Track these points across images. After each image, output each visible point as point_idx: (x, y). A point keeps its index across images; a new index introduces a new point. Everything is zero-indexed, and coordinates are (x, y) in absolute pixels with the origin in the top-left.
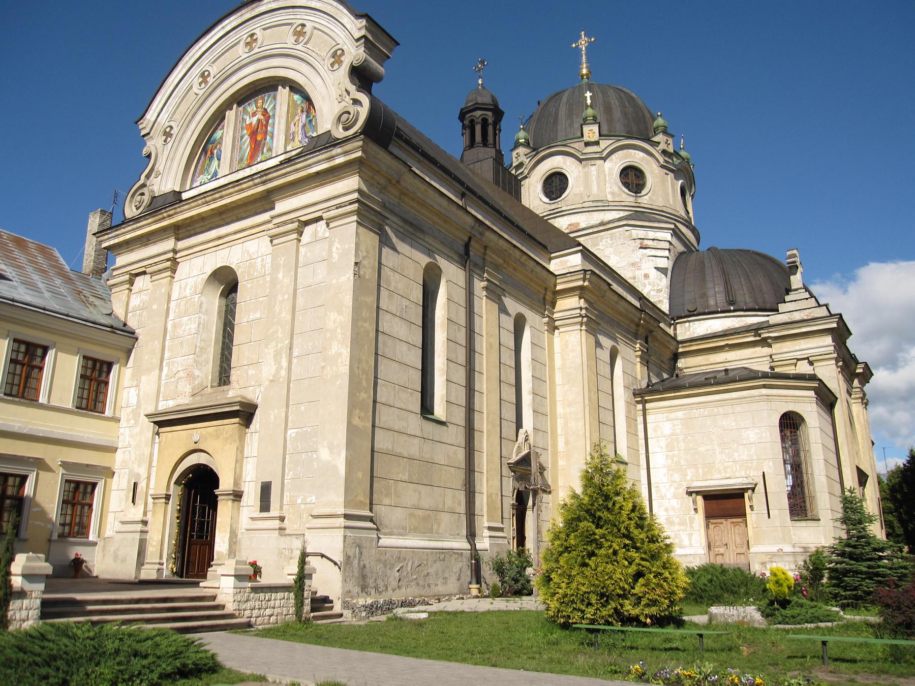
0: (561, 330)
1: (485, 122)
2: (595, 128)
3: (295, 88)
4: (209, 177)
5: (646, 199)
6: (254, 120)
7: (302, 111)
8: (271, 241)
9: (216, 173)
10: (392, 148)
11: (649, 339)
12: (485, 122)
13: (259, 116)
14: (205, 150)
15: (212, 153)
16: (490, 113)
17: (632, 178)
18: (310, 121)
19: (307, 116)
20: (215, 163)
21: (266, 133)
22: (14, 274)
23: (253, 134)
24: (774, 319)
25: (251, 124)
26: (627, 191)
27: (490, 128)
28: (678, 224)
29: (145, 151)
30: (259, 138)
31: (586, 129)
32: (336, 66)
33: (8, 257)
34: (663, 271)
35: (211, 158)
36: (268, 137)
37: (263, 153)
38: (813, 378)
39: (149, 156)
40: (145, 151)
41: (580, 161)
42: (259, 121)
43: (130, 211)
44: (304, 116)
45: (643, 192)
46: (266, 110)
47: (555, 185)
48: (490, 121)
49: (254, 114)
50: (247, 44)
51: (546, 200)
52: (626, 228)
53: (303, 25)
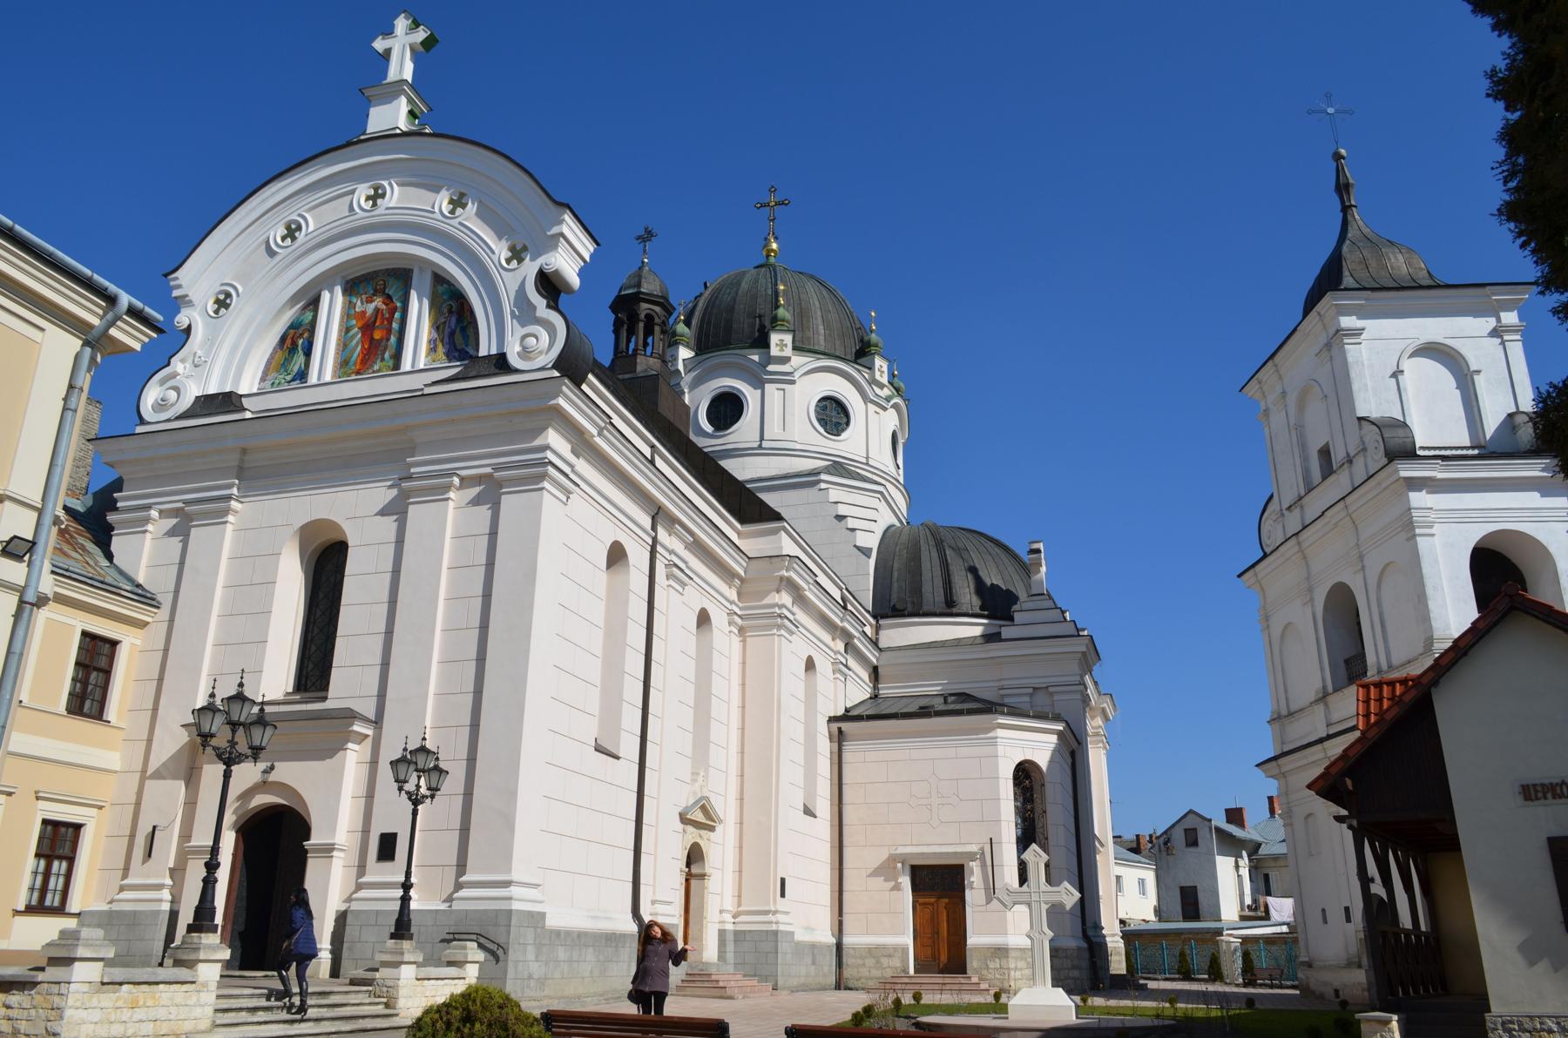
2: (788, 338)
3: (440, 280)
4: (289, 378)
5: (849, 445)
6: (370, 308)
7: (450, 312)
9: (302, 376)
10: (584, 387)
12: (649, 318)
14: (283, 339)
15: (294, 344)
16: (657, 309)
17: (833, 415)
18: (463, 330)
19: (459, 320)
21: (389, 331)
23: (368, 328)
25: (364, 313)
28: (889, 486)
30: (377, 335)
31: (775, 338)
32: (514, 263)
34: (866, 552)
35: (293, 349)
36: (393, 339)
37: (383, 359)
39: (188, 330)
42: (377, 310)
44: (454, 319)
45: (844, 435)
50: (368, 198)
52: (823, 486)
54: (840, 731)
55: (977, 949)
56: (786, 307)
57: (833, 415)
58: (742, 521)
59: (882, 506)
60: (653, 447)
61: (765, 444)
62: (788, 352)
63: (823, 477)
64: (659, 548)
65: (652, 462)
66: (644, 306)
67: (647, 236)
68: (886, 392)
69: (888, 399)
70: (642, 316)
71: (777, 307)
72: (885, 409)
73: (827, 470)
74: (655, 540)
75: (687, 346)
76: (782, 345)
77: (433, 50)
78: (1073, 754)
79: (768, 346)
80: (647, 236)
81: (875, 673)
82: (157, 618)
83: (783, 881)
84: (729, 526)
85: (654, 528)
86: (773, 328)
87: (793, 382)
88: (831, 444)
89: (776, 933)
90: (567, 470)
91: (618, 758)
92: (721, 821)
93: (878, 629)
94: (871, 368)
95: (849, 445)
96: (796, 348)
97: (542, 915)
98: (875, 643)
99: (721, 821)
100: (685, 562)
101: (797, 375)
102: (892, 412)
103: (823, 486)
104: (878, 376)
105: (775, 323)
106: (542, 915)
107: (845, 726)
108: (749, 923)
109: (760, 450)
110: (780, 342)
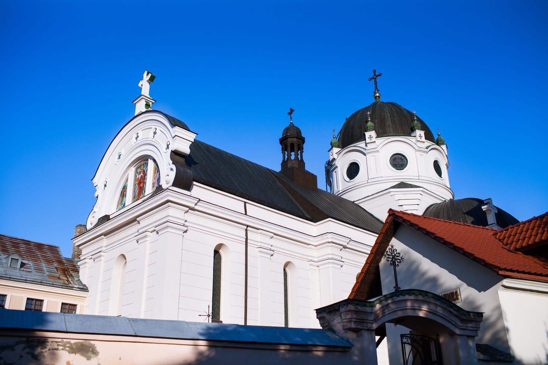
0: (321, 267)
1: (292, 145)
3: (155, 161)
6: (140, 175)
8: (138, 242)
12: (292, 145)
13: (142, 174)
16: (295, 140)
17: (399, 162)
20: (124, 199)
22: (32, 265)
26: (394, 169)
29: (96, 195)
31: (367, 134)
33: (31, 256)
35: (123, 196)
40: (96, 195)
41: (365, 154)
42: (141, 176)
43: (89, 227)
47: (353, 170)
48: (295, 145)
49: (140, 173)
51: (348, 179)
52: (392, 194)
60: (245, 203)
62: (374, 139)
64: (248, 241)
66: (289, 140)
67: (292, 111)
70: (289, 144)
74: (247, 239)
75: (338, 147)
76: (370, 137)
77: (154, 81)
80: (292, 111)
82: (89, 295)
86: (366, 131)
96: (379, 136)
101: (378, 149)
103: (392, 194)
109: (368, 183)
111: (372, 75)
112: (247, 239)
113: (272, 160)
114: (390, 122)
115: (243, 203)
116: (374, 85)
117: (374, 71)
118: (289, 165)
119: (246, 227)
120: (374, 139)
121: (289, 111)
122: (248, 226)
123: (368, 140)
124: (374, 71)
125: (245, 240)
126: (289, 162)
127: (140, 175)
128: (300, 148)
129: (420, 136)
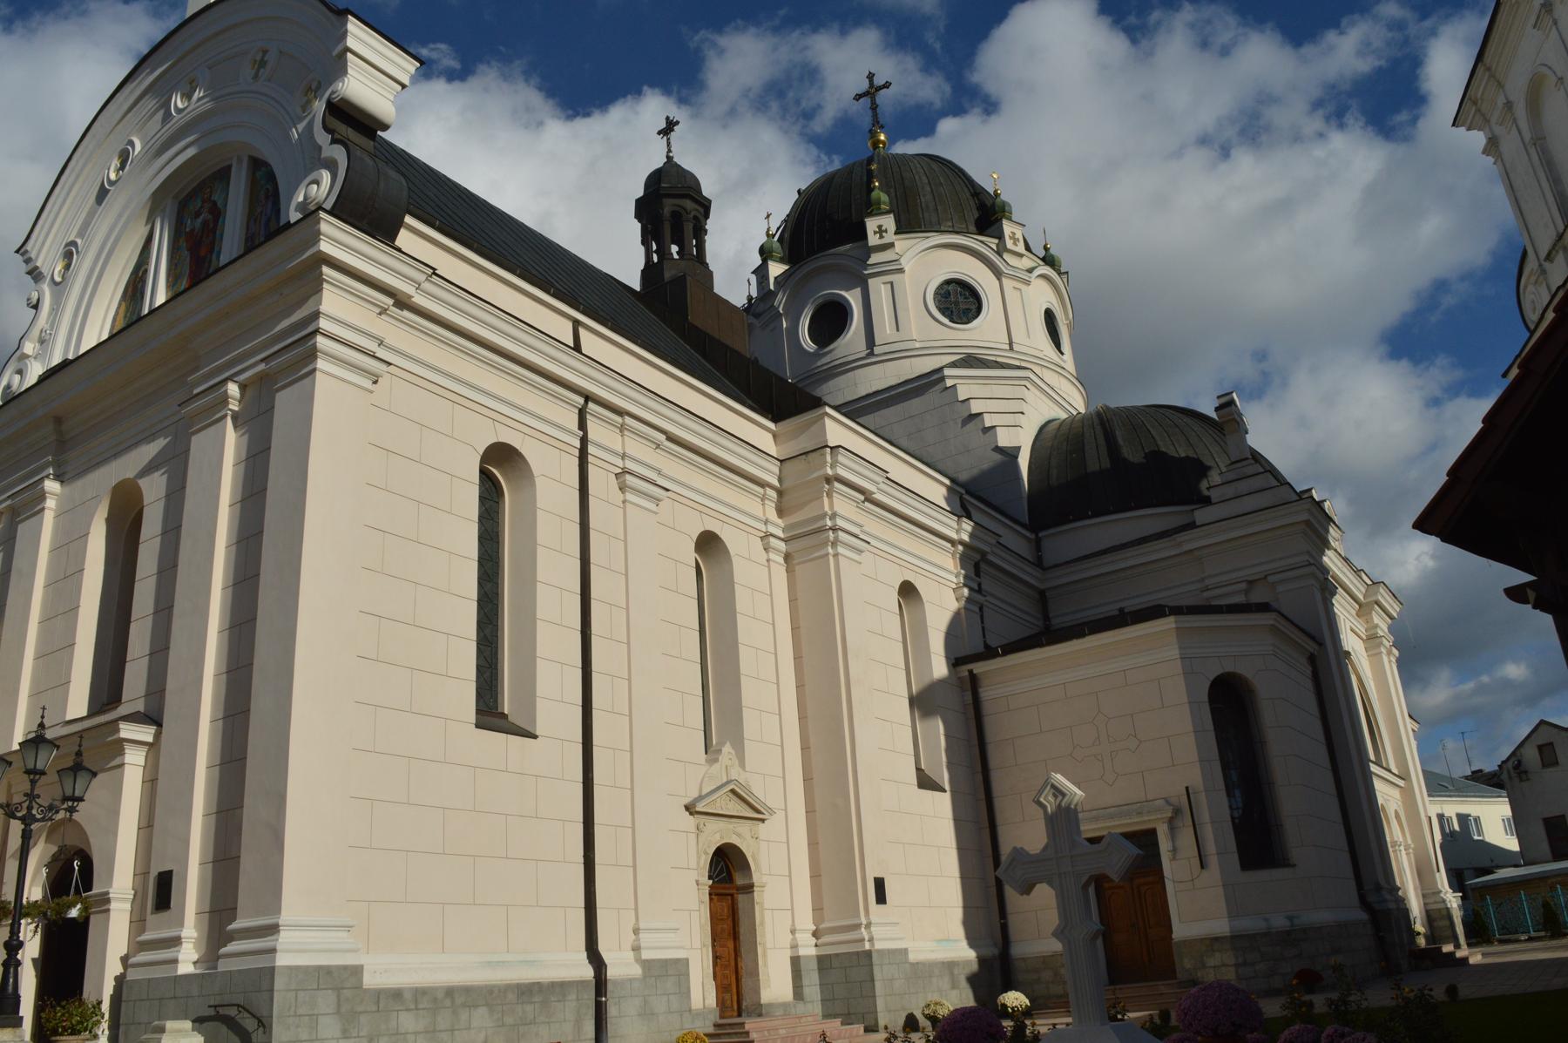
2: (889, 222)
6: (199, 220)
10: (404, 239)
11: (983, 566)
13: (205, 215)
23: (194, 247)
24: (1202, 515)
25: (192, 230)
26: (946, 321)
27: (689, 228)
31: (871, 224)
38: (1264, 608)
42: (205, 223)
46: (215, 203)
49: (198, 214)
53: (265, 52)
54: (972, 675)
55: (1185, 943)
56: (881, 188)
57: (959, 301)
58: (775, 420)
59: (1032, 395)
60: (577, 324)
61: (877, 350)
62: (890, 237)
63: (947, 372)
64: (591, 449)
65: (577, 347)
68: (1027, 262)
69: (1030, 271)
71: (872, 190)
72: (1027, 283)
73: (953, 365)
74: (584, 441)
75: (782, 261)
76: (881, 231)
78: (1312, 659)
79: (864, 236)
81: (1042, 598)
83: (880, 884)
84: (756, 430)
85: (582, 425)
86: (871, 215)
87: (901, 271)
88: (960, 335)
89: (869, 954)
90: (371, 345)
91: (535, 737)
92: (772, 812)
93: (1038, 545)
94: (1000, 236)
95: (984, 332)
97: (357, 971)
98: (1039, 563)
99: (772, 812)
100: (659, 472)
102: (1043, 284)
103: (949, 383)
104: (1009, 244)
105: (872, 209)
106: (357, 971)
107: (979, 668)
108: (837, 944)
110: (880, 226)
111: (865, 85)
112: (584, 441)
113: (621, 256)
114: (929, 197)
115: (570, 325)
116: (870, 112)
117: (871, 76)
118: (668, 275)
119: (581, 401)
120: (890, 237)
121: (663, 125)
122: (588, 398)
123: (873, 240)
124: (871, 76)
125: (578, 444)
126: (666, 265)
127: (199, 220)
128: (700, 232)
129: (1013, 237)
